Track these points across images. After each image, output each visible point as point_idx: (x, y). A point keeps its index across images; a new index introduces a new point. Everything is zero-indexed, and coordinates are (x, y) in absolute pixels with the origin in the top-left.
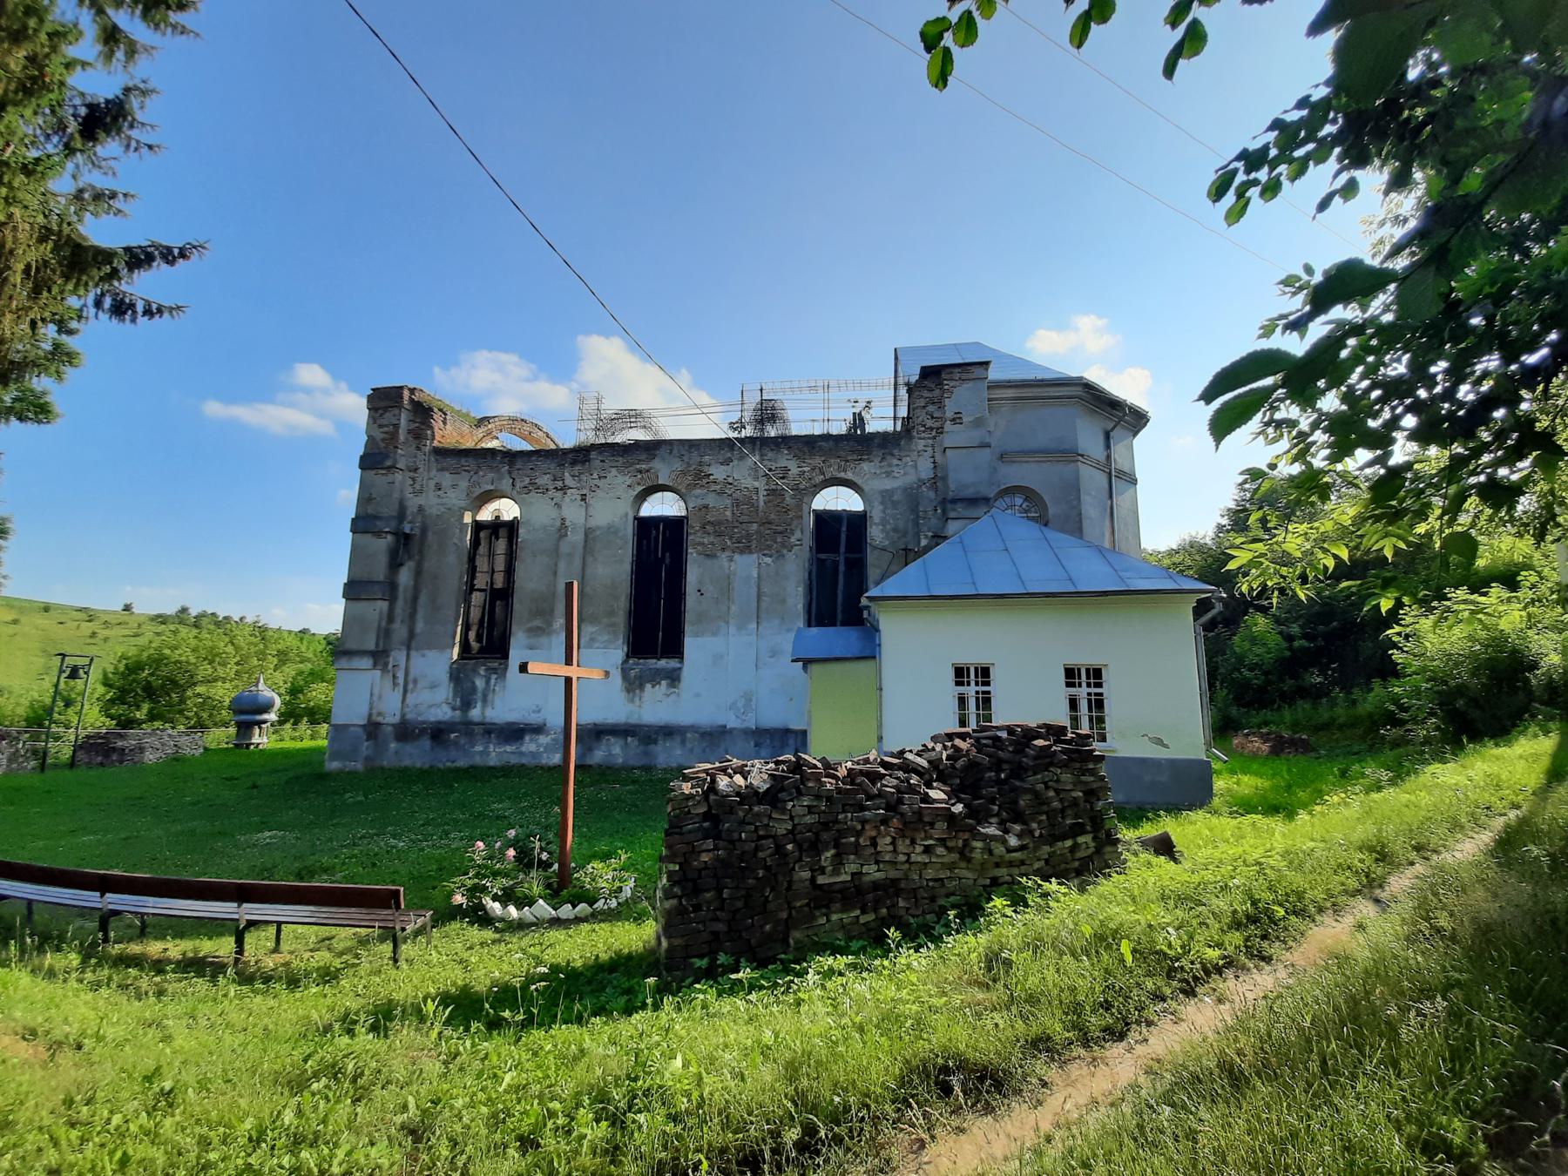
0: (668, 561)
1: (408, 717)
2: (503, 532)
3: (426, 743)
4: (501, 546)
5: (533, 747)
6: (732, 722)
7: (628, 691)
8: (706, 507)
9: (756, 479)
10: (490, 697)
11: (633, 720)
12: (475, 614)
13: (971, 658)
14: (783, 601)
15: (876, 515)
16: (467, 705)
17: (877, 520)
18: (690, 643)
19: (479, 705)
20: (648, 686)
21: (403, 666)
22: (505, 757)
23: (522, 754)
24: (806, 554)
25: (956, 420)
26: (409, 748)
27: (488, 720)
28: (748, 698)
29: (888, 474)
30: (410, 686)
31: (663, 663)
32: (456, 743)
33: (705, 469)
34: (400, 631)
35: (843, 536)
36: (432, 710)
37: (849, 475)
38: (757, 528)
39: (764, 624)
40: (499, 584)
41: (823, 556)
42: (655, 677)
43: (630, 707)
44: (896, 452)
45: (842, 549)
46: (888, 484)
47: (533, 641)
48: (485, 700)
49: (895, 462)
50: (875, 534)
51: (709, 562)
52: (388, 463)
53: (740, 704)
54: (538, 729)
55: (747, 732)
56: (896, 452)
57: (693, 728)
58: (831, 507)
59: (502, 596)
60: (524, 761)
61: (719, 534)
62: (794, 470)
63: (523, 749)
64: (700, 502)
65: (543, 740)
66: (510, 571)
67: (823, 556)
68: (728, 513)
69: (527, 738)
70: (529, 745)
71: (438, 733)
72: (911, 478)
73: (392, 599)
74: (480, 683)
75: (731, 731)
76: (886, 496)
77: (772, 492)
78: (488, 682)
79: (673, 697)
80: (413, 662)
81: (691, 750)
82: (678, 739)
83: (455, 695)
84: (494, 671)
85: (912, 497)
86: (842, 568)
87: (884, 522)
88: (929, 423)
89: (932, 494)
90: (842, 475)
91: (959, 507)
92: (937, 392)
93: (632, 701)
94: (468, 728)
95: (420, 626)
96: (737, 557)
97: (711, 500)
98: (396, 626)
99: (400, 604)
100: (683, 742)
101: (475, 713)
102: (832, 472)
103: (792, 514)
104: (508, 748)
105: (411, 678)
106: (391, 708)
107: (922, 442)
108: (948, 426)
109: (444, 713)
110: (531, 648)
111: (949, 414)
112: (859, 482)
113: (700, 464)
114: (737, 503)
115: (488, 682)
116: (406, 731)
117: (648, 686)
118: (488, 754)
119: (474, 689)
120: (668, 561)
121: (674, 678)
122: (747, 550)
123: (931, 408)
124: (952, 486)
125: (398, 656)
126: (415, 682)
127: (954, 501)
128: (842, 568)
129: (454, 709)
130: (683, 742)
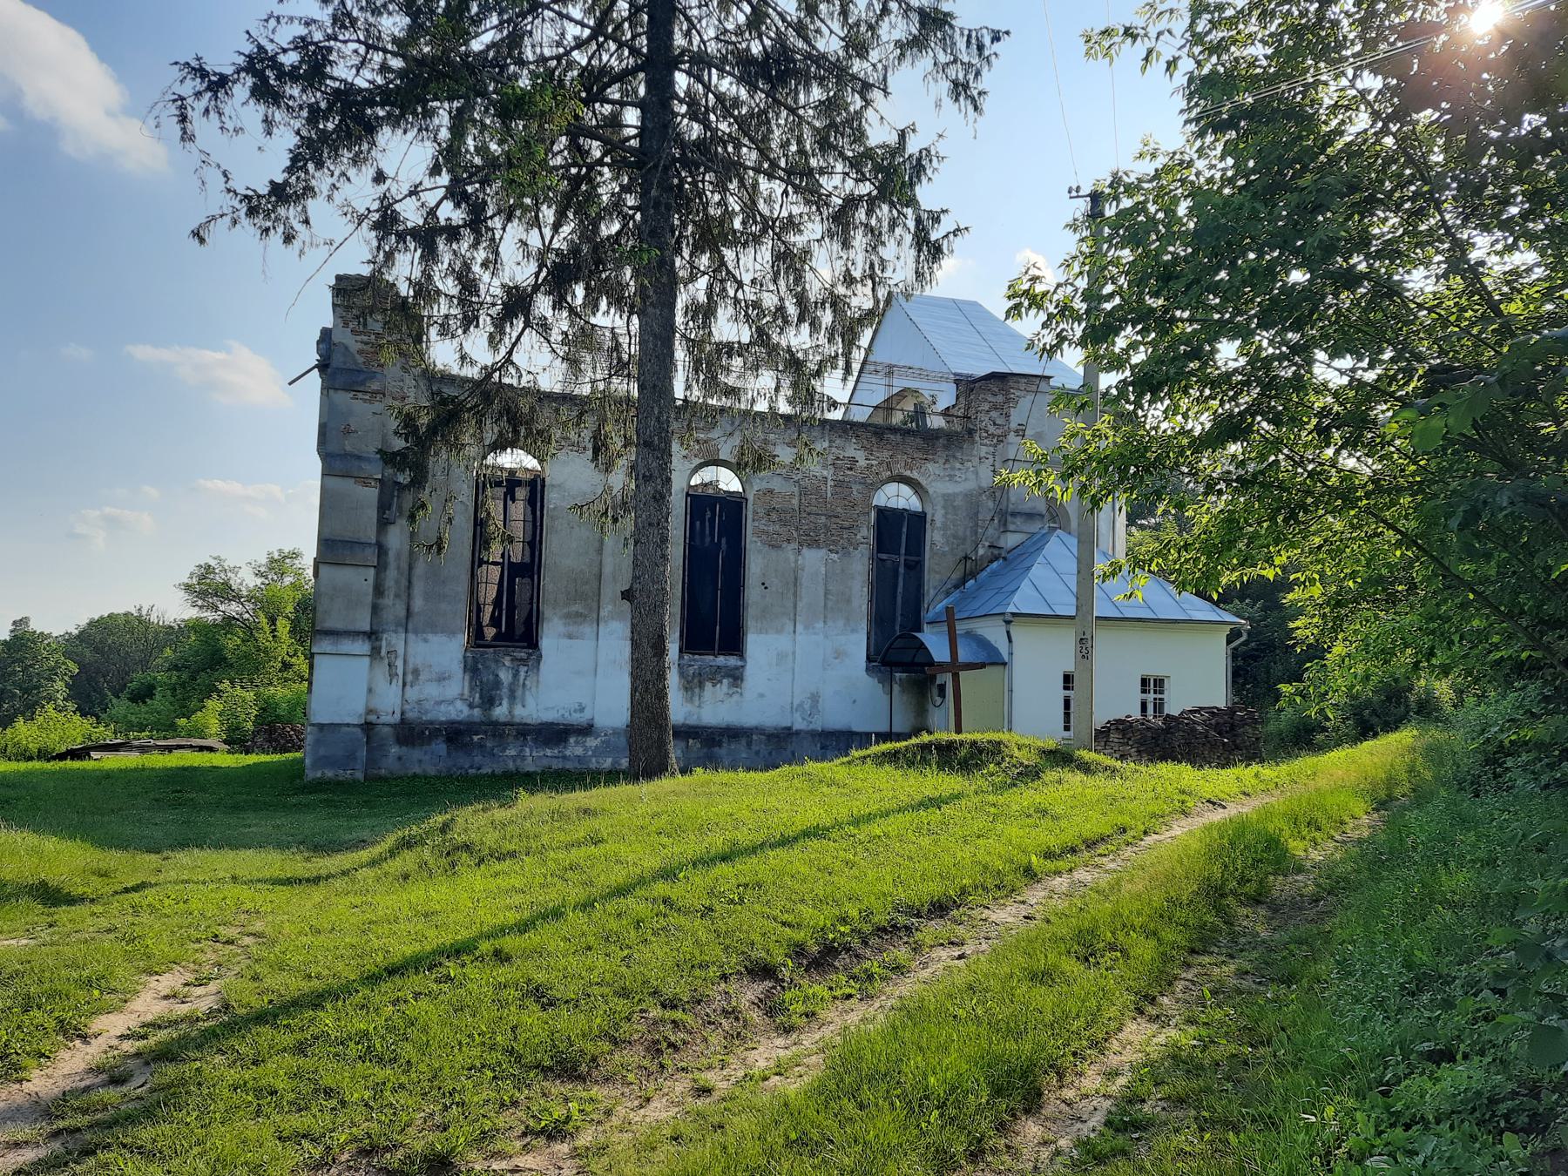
0: (724, 546)
1: (410, 715)
2: (521, 493)
3: (440, 747)
4: (518, 509)
5: (579, 751)
6: (799, 724)
7: (686, 689)
8: (771, 491)
9: (825, 467)
10: (519, 693)
11: (692, 721)
12: (489, 593)
13: (1154, 671)
14: (849, 601)
15: (937, 515)
16: (489, 701)
17: (938, 524)
18: (754, 642)
19: (505, 702)
20: (708, 685)
21: (401, 652)
22: (545, 762)
23: (564, 757)
24: (867, 553)
25: (1021, 432)
26: (416, 754)
27: (517, 720)
28: (815, 698)
29: (951, 477)
30: (409, 678)
31: (721, 660)
32: (481, 746)
33: (770, 448)
34: (393, 608)
35: (904, 537)
36: (443, 708)
37: (915, 475)
38: (811, 524)
39: (830, 623)
40: (517, 553)
41: (884, 556)
42: (716, 675)
43: (689, 707)
44: (958, 455)
45: (903, 551)
46: (950, 488)
47: (571, 628)
48: (512, 697)
49: (958, 465)
50: (935, 537)
51: (774, 554)
52: (375, 386)
53: (807, 706)
54: (587, 730)
55: (814, 734)
56: (958, 455)
57: (759, 730)
58: (892, 504)
59: (525, 570)
60: (569, 765)
61: (784, 523)
62: (862, 463)
63: (568, 753)
64: (764, 485)
65: (592, 742)
66: (534, 543)
67: (884, 556)
68: (795, 502)
69: (572, 740)
70: (574, 748)
71: (455, 734)
72: (970, 485)
73: (381, 567)
74: (505, 676)
75: (798, 733)
76: (948, 499)
77: (839, 484)
78: (516, 675)
79: (736, 697)
80: (411, 643)
81: (757, 753)
82: (744, 742)
83: (472, 689)
84: (523, 662)
85: (972, 503)
86: (902, 570)
87: (945, 527)
88: (992, 429)
89: (991, 504)
90: (908, 473)
91: (1018, 521)
92: (1000, 398)
93: (691, 700)
94: (497, 730)
95: (418, 603)
96: (805, 550)
97: (777, 484)
98: (388, 601)
99: (391, 574)
100: (749, 744)
101: (500, 712)
102: (899, 469)
103: (859, 509)
104: (549, 752)
105: (410, 667)
106: (389, 702)
107: (984, 449)
108: (1012, 437)
109: (459, 711)
110: (570, 637)
111: (1013, 425)
112: (924, 483)
113: (766, 441)
114: (804, 492)
115: (516, 675)
116: (410, 732)
117: (708, 685)
118: (524, 758)
119: (497, 683)
120: (724, 546)
121: (736, 677)
122: (814, 544)
123: (994, 414)
124: (1013, 499)
125: (394, 640)
126: (416, 672)
127: (1014, 514)
128: (902, 570)
129: (471, 706)
130: (749, 744)
